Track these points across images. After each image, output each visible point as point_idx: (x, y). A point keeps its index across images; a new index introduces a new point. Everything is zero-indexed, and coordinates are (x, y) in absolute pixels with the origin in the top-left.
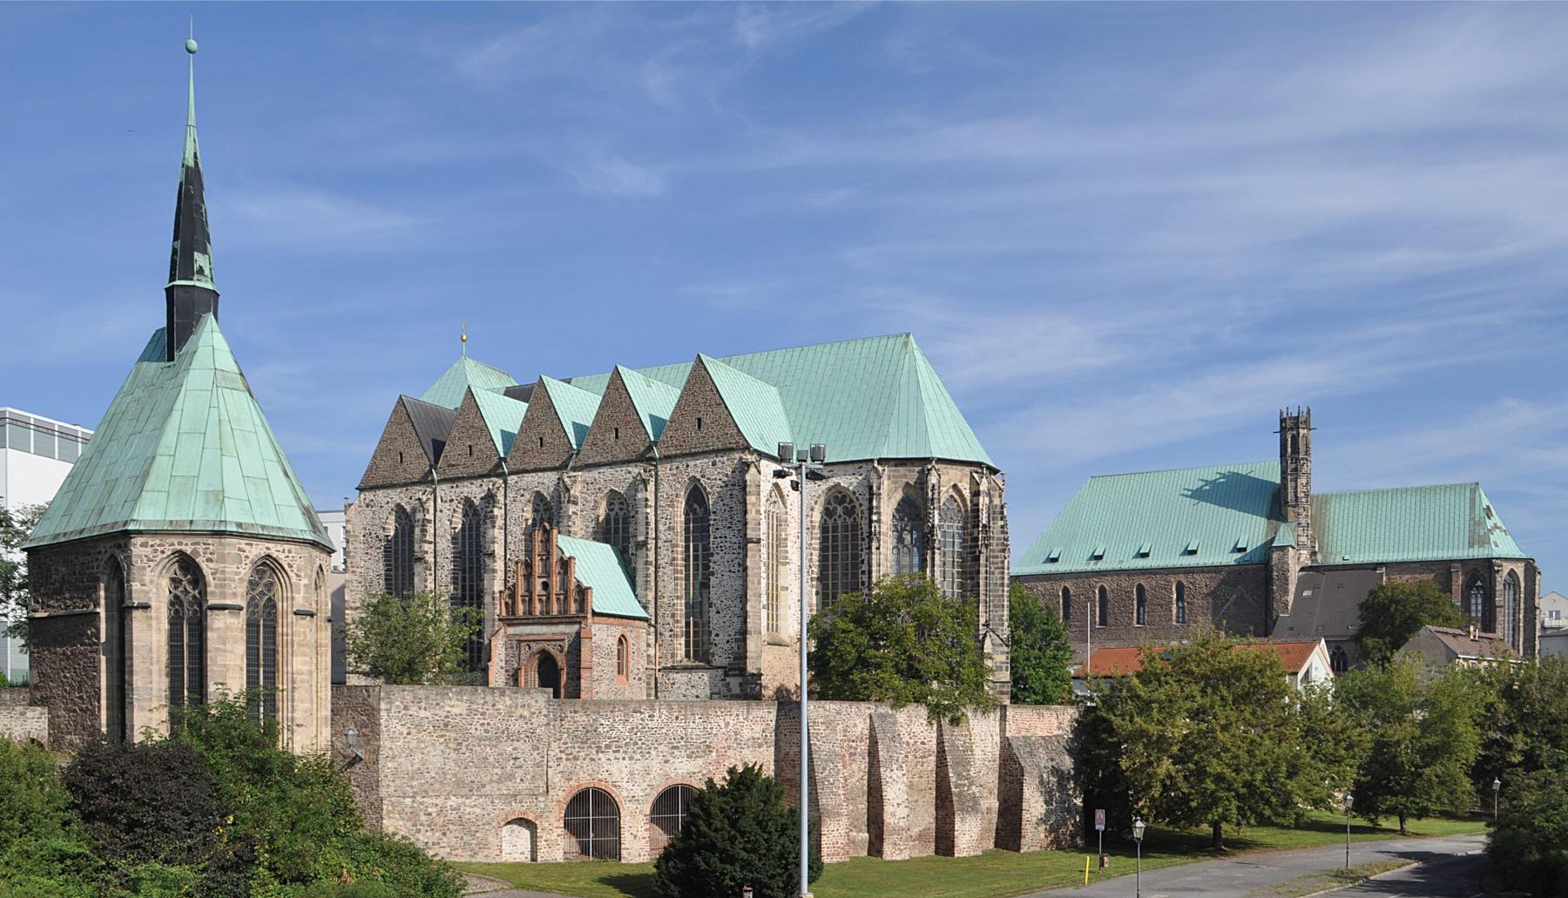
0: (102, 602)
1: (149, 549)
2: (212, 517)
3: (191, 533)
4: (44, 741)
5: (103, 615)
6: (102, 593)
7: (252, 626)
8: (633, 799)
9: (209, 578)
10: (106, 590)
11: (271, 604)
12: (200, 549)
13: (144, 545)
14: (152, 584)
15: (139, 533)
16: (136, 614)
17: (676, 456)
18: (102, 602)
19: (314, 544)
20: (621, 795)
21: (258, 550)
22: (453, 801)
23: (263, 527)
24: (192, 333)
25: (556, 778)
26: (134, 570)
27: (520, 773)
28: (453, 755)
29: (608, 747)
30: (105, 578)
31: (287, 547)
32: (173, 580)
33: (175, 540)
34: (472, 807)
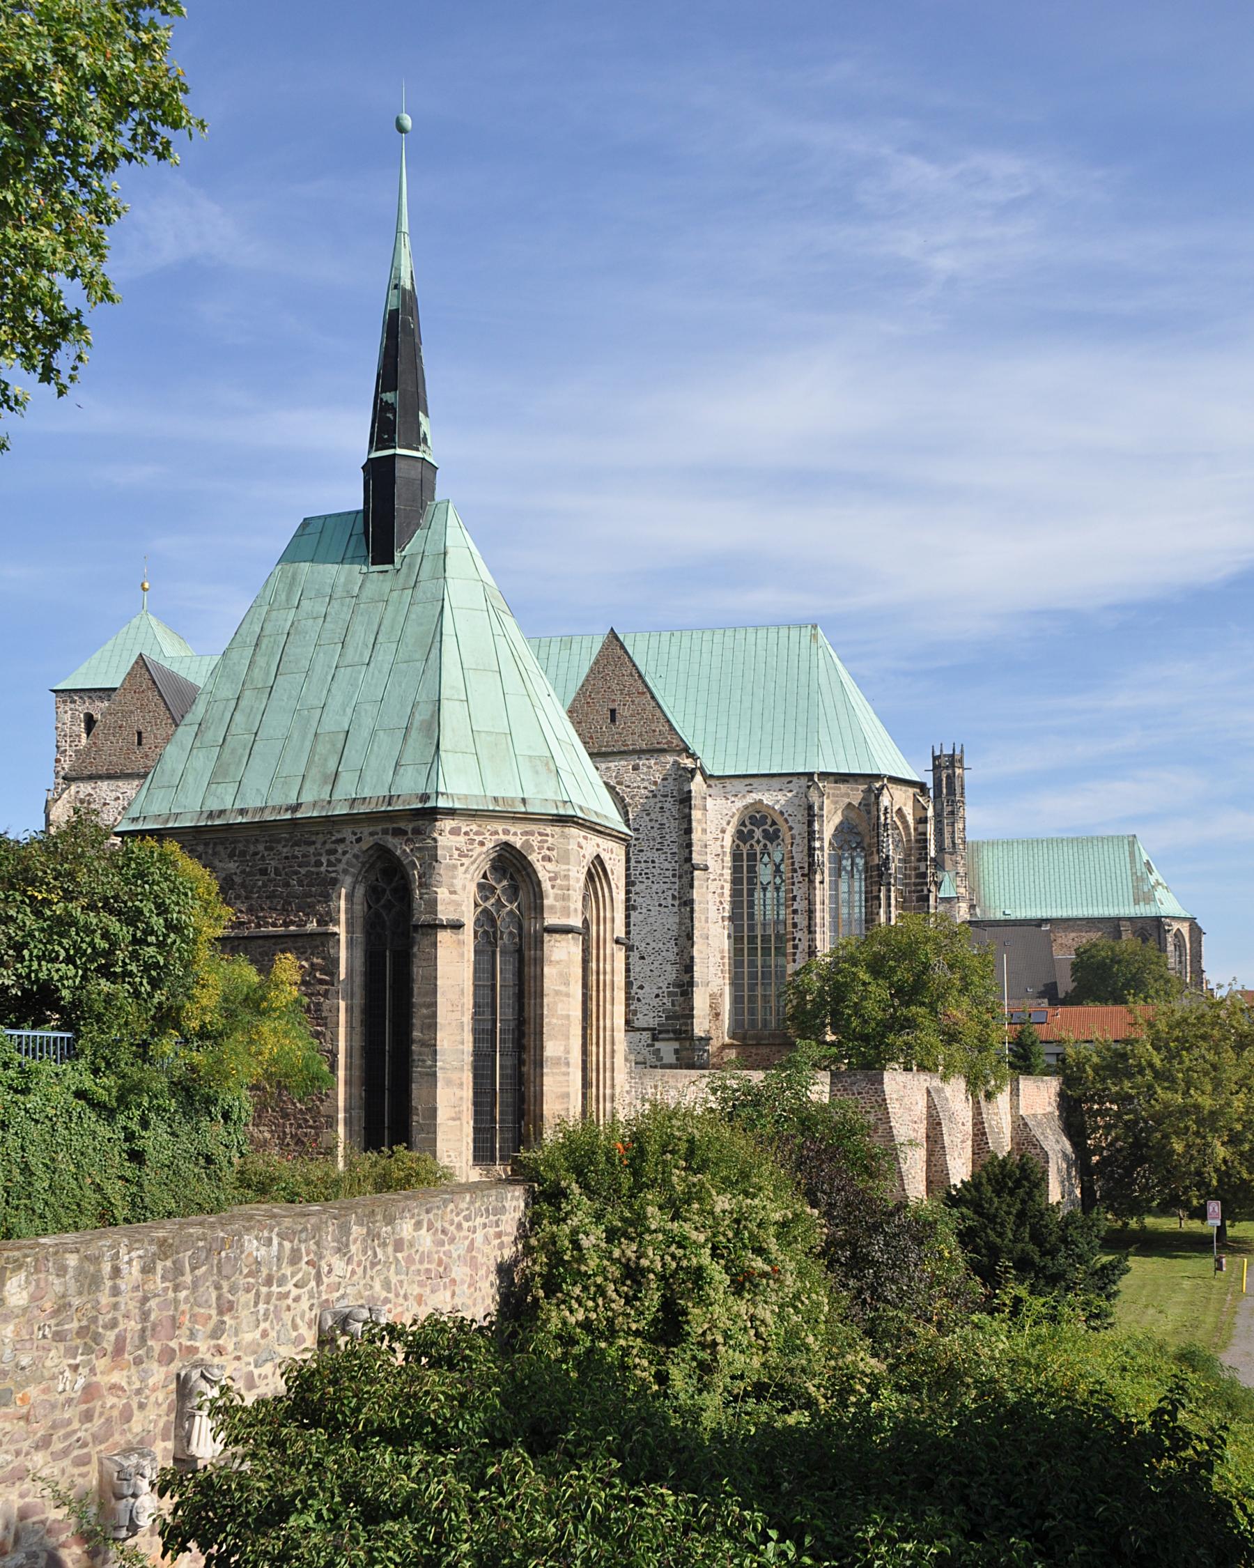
0: (343, 917)
1: (462, 838)
2: (550, 795)
3: (527, 818)
5: (343, 938)
6: (343, 904)
9: (546, 885)
10: (350, 898)
12: (535, 841)
13: (455, 832)
14: (457, 890)
15: (451, 812)
16: (443, 936)
18: (343, 917)
26: (441, 869)
30: (348, 880)
32: (480, 886)
33: (499, 826)
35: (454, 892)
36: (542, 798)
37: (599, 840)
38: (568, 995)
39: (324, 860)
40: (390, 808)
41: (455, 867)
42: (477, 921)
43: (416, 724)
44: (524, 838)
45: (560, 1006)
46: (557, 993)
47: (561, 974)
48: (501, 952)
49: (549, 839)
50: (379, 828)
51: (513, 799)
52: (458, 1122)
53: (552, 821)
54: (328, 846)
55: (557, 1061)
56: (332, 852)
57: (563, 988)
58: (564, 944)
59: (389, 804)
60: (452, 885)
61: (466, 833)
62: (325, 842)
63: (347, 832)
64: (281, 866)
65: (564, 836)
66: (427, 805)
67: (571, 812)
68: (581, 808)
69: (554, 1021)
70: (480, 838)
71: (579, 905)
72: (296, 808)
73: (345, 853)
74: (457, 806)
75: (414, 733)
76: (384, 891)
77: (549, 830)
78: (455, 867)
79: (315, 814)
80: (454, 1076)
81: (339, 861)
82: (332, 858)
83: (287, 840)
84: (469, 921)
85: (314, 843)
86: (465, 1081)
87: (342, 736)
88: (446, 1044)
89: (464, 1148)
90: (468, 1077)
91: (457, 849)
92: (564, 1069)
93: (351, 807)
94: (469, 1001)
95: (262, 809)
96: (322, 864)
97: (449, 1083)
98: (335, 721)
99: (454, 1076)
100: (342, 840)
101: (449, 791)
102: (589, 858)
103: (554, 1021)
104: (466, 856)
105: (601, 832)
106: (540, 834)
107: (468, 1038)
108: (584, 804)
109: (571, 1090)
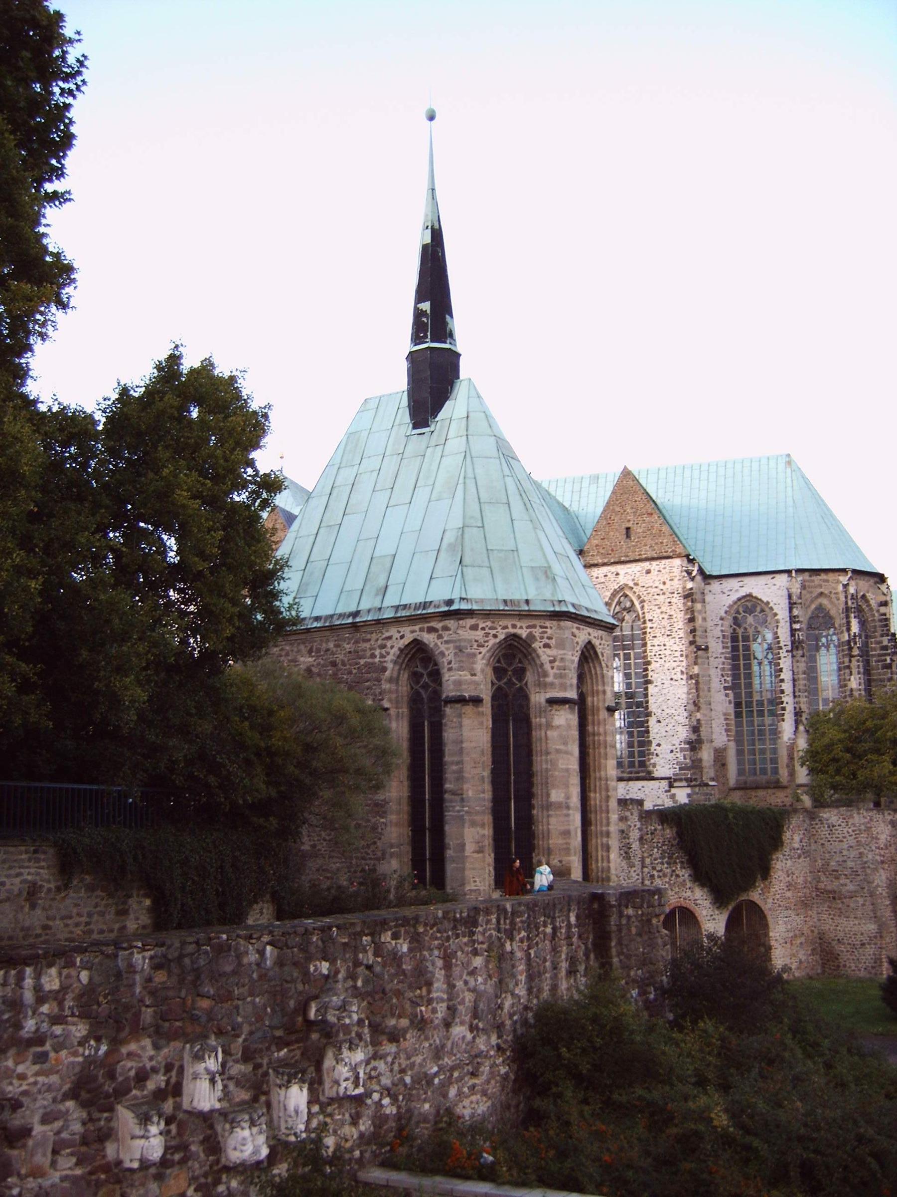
2: (548, 596)
4: (268, 897)
9: (547, 666)
12: (537, 632)
13: (474, 628)
24: (446, 398)
33: (508, 622)
35: (474, 675)
36: (539, 596)
37: (590, 630)
38: (567, 753)
39: (377, 652)
40: (424, 612)
41: (474, 655)
42: (494, 698)
43: (444, 546)
44: (529, 630)
45: (560, 762)
46: (558, 751)
47: (560, 736)
48: (514, 720)
49: (548, 630)
50: (417, 628)
51: (519, 601)
52: (481, 855)
53: (550, 616)
54: (380, 642)
55: (559, 806)
56: (383, 647)
57: (562, 747)
58: (562, 712)
59: (424, 609)
60: (473, 669)
61: (483, 629)
62: (377, 640)
63: (393, 631)
64: (346, 659)
65: (559, 627)
66: (452, 608)
67: (564, 609)
68: (573, 605)
69: (557, 773)
70: (494, 632)
71: (575, 681)
72: (356, 614)
73: (392, 647)
74: (475, 607)
75: (443, 554)
76: (422, 675)
77: (548, 624)
78: (474, 655)
79: (369, 619)
80: (478, 818)
81: (388, 653)
82: (383, 652)
83: (350, 639)
84: (487, 697)
85: (369, 640)
86: (486, 821)
87: (389, 559)
88: (470, 793)
89: (487, 876)
90: (488, 819)
91: (476, 641)
92: (565, 812)
93: (396, 612)
94: (488, 759)
95: (332, 616)
96: (376, 657)
97: (473, 824)
98: (385, 548)
99: (478, 818)
100: (390, 638)
101: (469, 597)
102: (582, 644)
103: (557, 773)
104: (483, 646)
105: (590, 623)
106: (541, 627)
107: (488, 787)
108: (575, 601)
109: (572, 828)
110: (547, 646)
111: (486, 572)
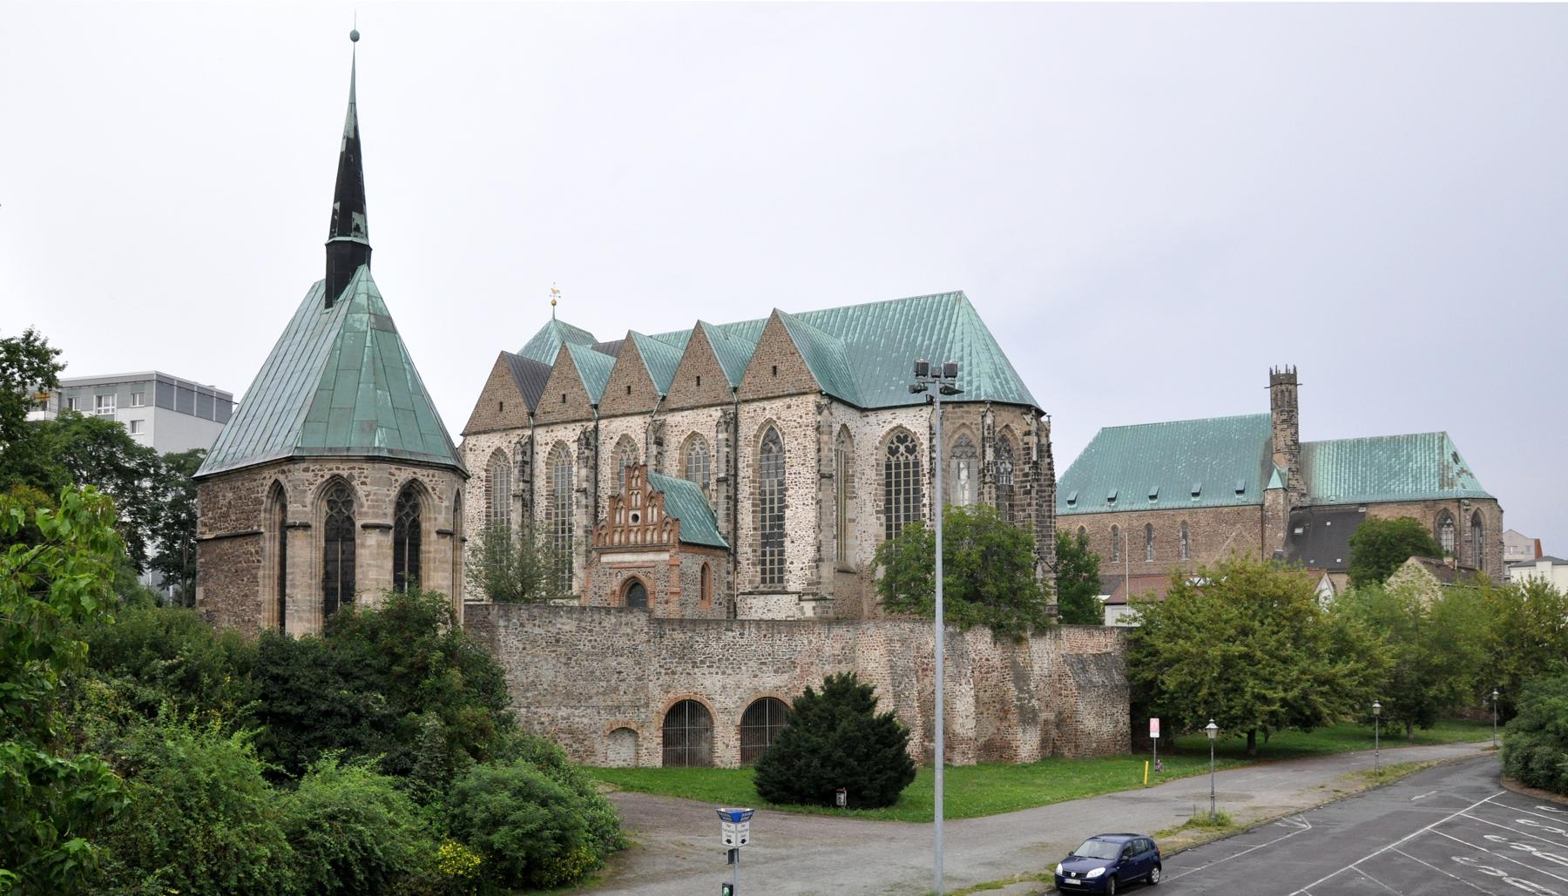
2: (366, 443)
3: (348, 459)
7: (398, 546)
8: (725, 710)
9: (364, 499)
11: (416, 525)
12: (356, 473)
13: (306, 470)
17: (753, 400)
19: (453, 469)
20: (713, 707)
21: (405, 475)
22: (564, 712)
23: (411, 453)
25: (654, 688)
27: (623, 686)
28: (564, 669)
29: (702, 662)
31: (431, 472)
34: (581, 718)
77: (365, 466)
110: (363, 483)
111: (323, 426)
